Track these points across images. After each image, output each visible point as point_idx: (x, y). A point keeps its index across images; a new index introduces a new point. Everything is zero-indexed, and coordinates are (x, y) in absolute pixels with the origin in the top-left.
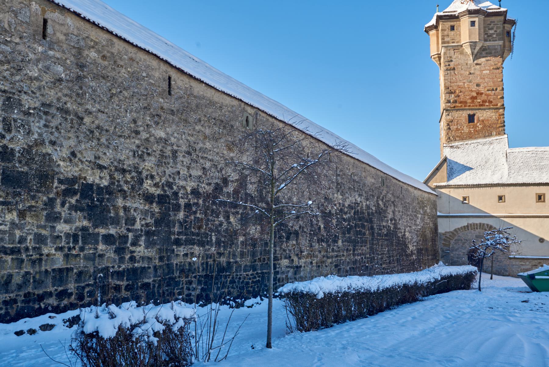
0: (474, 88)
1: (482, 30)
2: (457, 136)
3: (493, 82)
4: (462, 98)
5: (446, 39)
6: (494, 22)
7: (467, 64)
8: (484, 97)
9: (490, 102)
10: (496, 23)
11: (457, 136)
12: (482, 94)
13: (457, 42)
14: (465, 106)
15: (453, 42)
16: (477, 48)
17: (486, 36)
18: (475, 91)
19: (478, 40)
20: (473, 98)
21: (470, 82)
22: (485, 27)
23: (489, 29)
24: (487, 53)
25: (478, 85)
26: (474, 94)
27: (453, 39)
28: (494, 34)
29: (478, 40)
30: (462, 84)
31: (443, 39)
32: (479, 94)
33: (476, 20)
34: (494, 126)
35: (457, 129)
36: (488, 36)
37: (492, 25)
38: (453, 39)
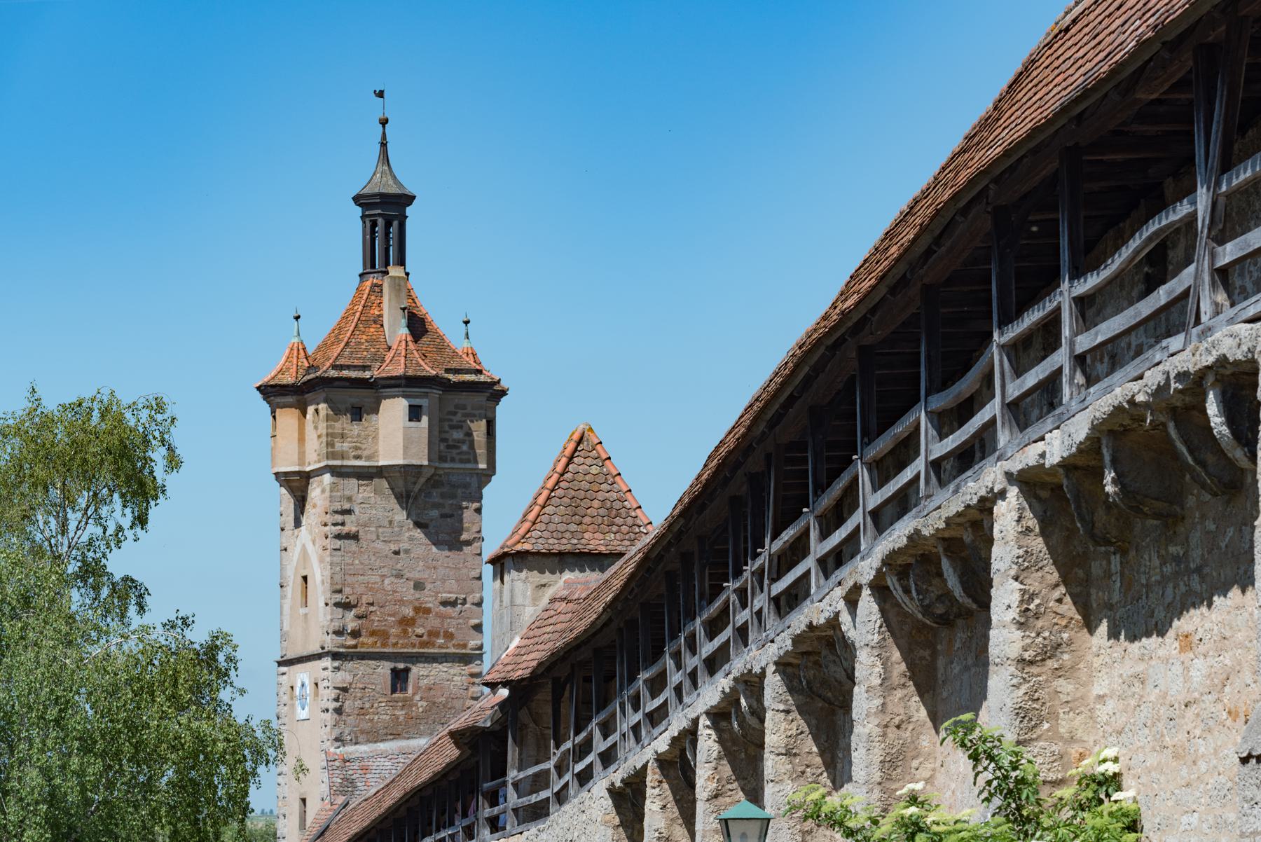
0: (409, 593)
1: (436, 433)
2: (362, 732)
3: (457, 581)
4: (376, 621)
5: (338, 446)
6: (464, 407)
7: (391, 522)
8: (433, 622)
9: (449, 636)
10: (469, 410)
11: (362, 732)
12: (428, 611)
13: (368, 458)
14: (384, 645)
15: (357, 457)
16: (422, 480)
17: (442, 447)
18: (411, 602)
19: (426, 463)
20: (406, 622)
21: (399, 576)
22: (441, 420)
23: (452, 427)
24: (443, 496)
25: (419, 586)
26: (408, 612)
27: (357, 448)
28: (463, 442)
29: (426, 463)
30: (378, 579)
31: (330, 444)
32: (422, 610)
33: (424, 402)
34: (458, 704)
35: (362, 711)
36: (448, 447)
37: (459, 417)
38: (357, 448)
